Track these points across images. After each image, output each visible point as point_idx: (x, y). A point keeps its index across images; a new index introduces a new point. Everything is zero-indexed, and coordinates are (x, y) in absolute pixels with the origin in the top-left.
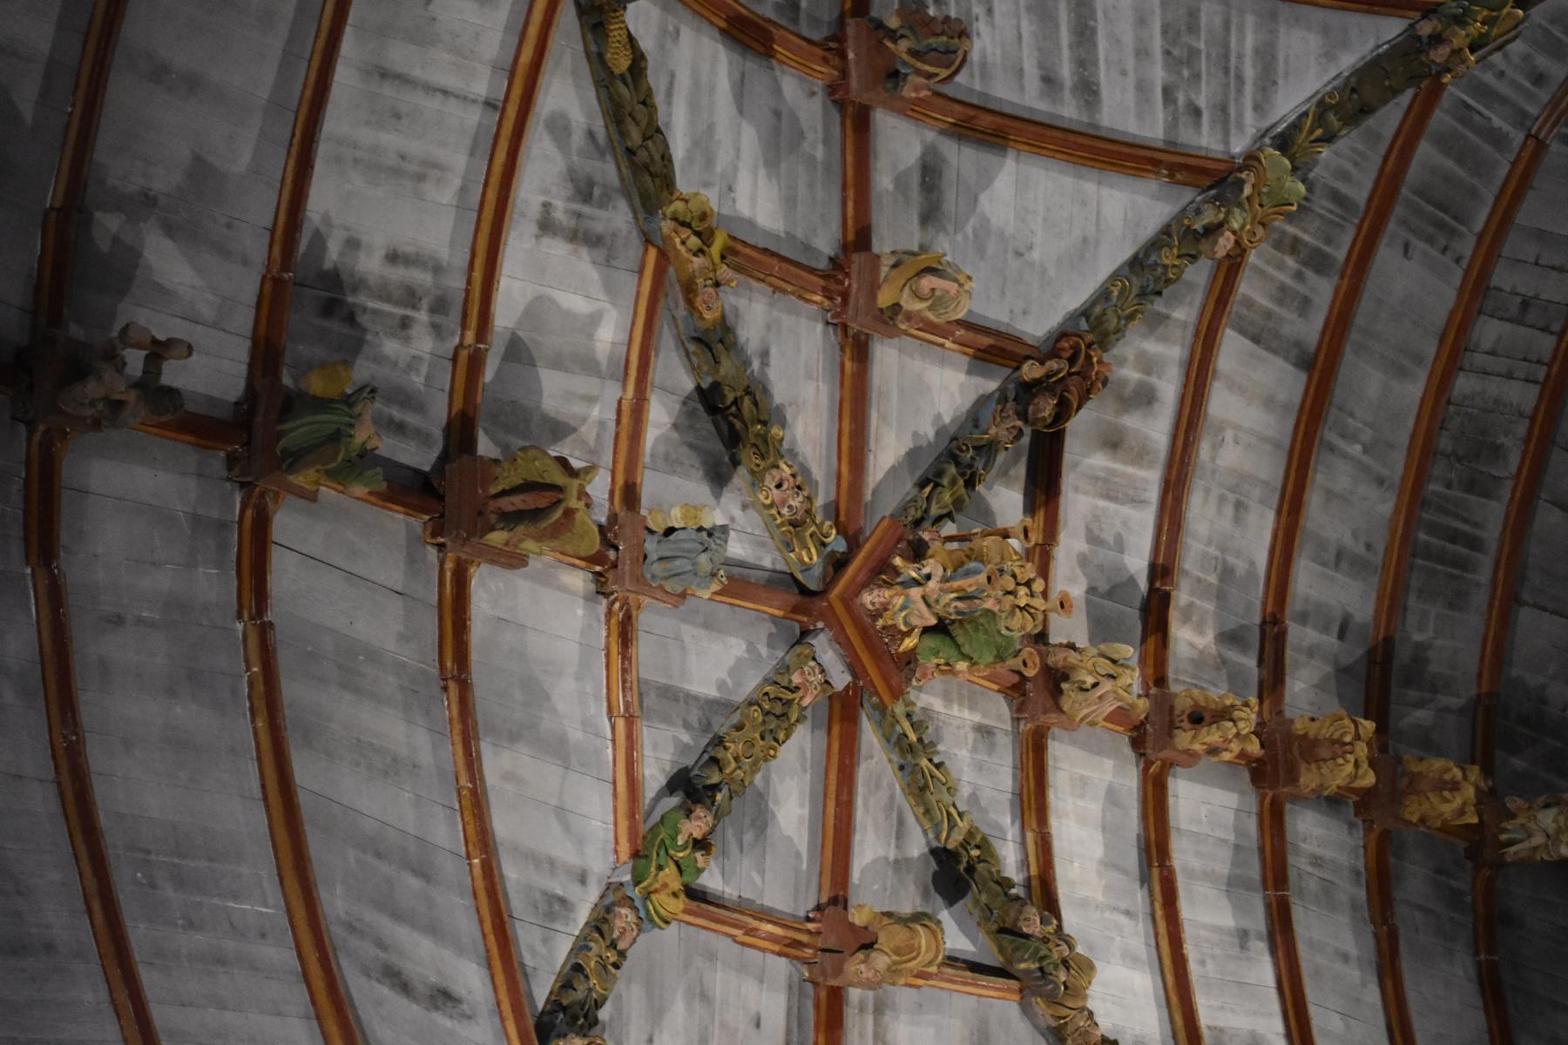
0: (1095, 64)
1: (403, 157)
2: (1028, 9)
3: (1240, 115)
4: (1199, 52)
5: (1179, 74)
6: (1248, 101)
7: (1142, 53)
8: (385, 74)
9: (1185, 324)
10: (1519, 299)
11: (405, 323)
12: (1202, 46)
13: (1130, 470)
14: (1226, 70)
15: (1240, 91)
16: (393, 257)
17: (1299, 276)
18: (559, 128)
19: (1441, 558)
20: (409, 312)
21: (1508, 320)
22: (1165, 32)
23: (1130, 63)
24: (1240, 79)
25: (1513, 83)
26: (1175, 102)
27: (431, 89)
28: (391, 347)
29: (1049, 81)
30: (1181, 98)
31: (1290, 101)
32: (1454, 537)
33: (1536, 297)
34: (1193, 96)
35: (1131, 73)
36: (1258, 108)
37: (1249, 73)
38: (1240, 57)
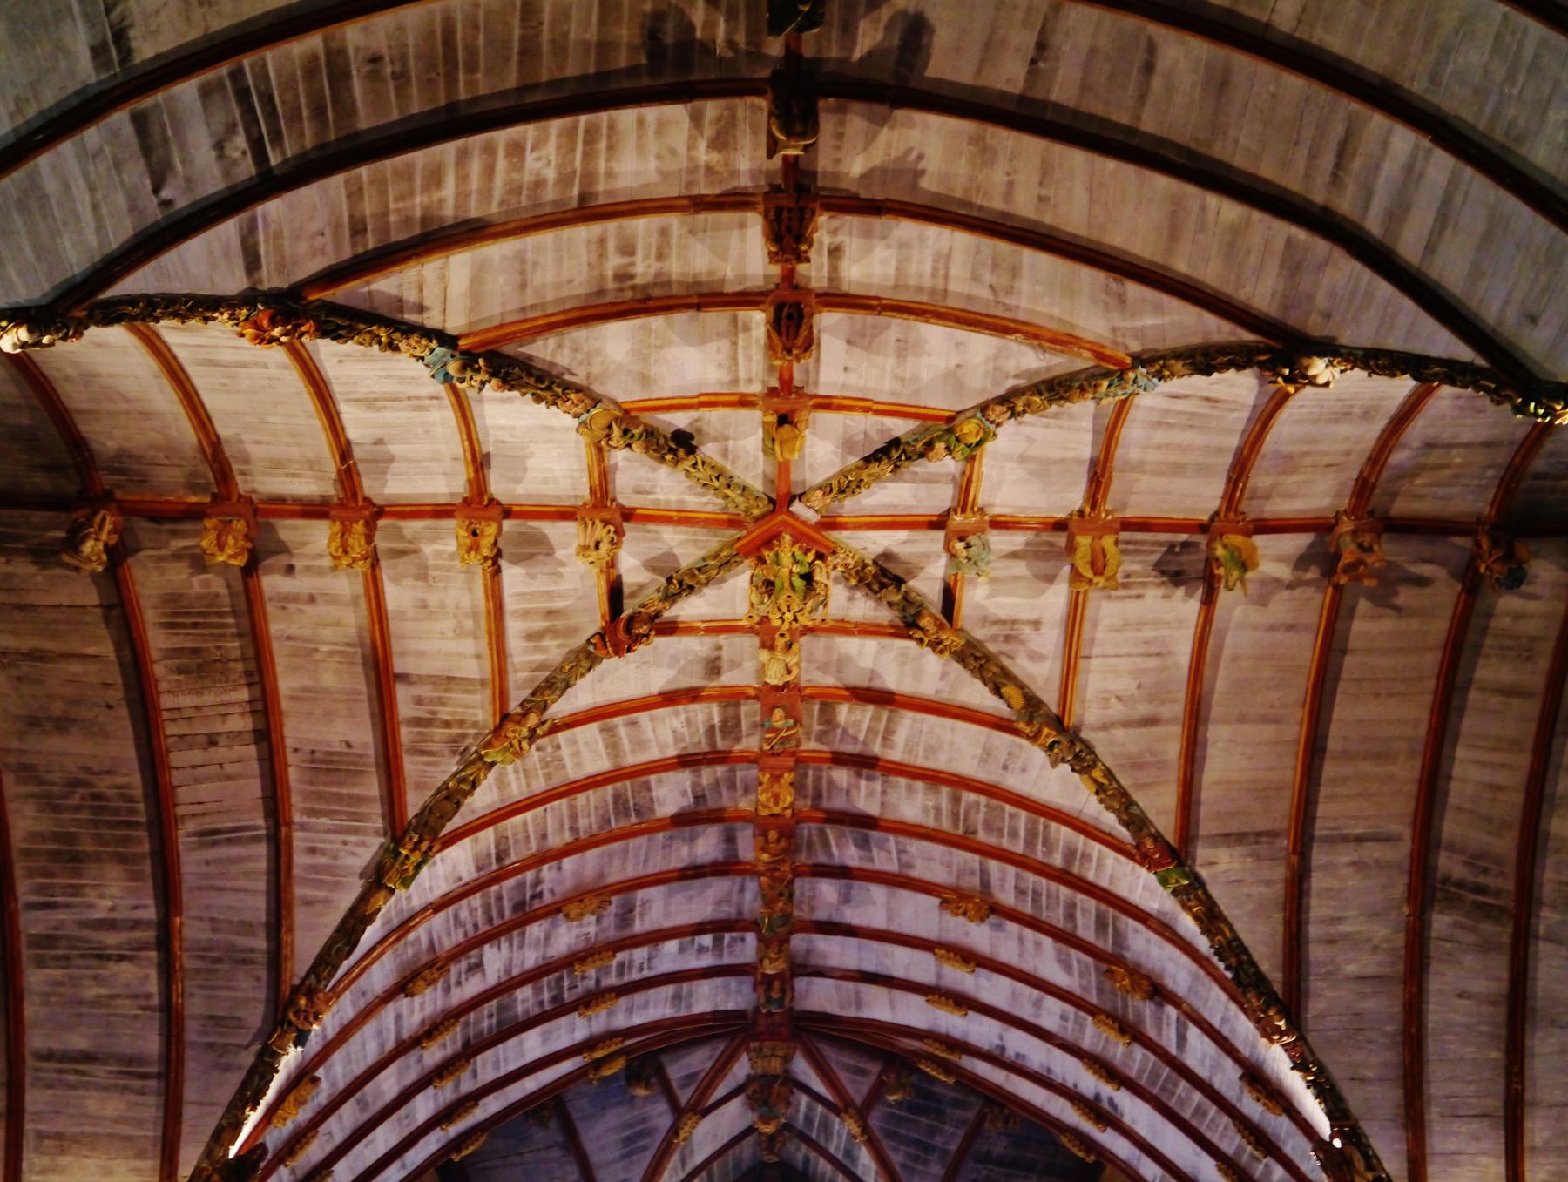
7: (577, 754)
8: (1158, 655)
9: (516, 671)
17: (433, 713)
18: (1035, 656)
19: (188, 614)
25: (331, 842)
27: (1130, 655)
28: (1136, 567)
32: (183, 626)
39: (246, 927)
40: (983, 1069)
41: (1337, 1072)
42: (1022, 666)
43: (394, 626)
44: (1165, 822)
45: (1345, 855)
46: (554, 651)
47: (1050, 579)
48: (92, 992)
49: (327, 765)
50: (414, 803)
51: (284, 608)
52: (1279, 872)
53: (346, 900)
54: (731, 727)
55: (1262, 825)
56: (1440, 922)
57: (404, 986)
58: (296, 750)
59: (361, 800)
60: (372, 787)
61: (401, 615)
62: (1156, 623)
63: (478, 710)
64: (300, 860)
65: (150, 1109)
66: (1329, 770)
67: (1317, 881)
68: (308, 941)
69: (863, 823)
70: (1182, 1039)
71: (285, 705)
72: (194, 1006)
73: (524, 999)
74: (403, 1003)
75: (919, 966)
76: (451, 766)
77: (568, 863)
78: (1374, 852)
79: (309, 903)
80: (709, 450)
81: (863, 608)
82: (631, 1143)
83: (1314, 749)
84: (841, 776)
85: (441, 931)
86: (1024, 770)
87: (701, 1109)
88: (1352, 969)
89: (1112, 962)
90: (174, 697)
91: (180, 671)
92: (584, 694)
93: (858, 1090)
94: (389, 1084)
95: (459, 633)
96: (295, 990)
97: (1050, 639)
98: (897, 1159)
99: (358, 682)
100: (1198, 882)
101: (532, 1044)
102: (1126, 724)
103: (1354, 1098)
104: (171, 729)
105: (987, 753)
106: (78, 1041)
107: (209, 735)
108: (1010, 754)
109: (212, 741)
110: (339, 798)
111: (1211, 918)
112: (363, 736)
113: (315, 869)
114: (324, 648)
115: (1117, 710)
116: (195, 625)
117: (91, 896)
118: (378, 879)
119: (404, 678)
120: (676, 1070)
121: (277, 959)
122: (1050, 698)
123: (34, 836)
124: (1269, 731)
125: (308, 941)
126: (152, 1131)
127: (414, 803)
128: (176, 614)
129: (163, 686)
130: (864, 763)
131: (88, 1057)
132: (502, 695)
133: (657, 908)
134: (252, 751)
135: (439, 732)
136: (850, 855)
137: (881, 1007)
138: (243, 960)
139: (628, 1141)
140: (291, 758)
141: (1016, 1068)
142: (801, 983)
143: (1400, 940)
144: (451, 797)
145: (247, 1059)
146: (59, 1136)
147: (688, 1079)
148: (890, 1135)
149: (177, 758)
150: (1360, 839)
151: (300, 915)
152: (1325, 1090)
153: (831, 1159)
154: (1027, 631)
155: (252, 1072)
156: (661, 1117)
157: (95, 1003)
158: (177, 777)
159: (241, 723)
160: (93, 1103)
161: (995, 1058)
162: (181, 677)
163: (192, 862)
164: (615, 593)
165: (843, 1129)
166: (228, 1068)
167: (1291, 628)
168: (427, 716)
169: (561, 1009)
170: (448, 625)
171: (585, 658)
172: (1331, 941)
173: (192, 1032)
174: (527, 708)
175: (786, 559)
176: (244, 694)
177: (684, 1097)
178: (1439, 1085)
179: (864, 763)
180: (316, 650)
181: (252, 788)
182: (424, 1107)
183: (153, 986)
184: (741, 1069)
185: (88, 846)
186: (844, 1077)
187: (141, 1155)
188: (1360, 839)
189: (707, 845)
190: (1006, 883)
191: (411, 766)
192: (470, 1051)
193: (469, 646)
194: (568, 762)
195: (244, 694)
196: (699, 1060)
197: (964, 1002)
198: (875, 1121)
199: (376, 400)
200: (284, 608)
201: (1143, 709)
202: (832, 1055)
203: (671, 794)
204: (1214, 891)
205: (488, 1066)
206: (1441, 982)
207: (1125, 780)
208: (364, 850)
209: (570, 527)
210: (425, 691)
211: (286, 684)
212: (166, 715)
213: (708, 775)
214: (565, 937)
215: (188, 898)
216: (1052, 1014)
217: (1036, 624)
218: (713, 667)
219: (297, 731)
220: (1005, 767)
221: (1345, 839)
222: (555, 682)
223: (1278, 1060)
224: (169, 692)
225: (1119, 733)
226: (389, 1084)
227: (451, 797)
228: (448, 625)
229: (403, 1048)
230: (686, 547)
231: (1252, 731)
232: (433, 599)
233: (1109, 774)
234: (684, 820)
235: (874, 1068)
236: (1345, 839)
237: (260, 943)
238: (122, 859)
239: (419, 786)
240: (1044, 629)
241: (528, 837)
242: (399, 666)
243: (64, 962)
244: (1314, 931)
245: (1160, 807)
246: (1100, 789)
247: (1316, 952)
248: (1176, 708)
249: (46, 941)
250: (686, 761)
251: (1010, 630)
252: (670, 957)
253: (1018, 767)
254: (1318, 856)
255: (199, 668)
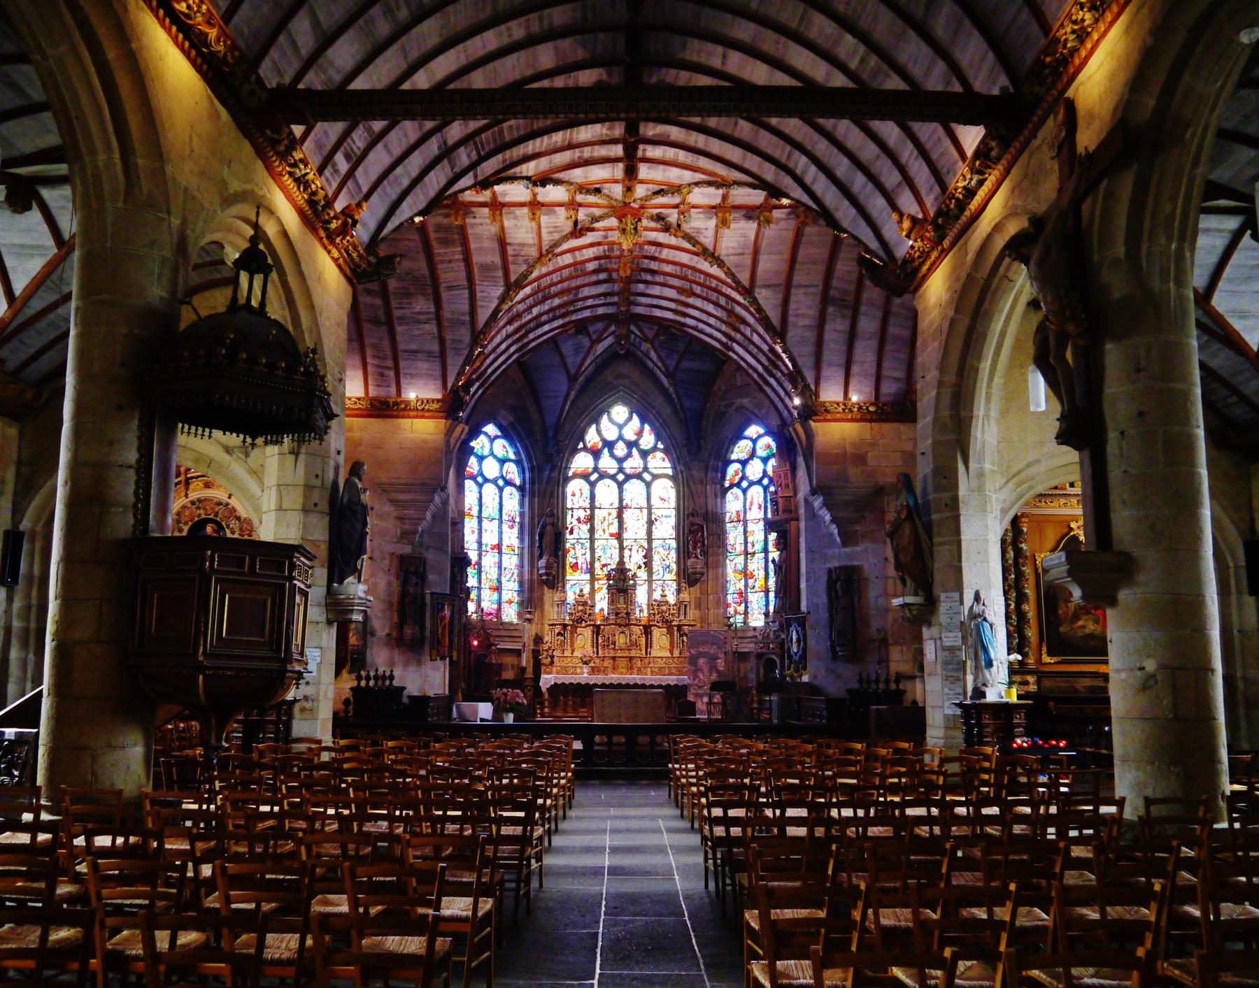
18: (705, 237)
39: (463, 314)
40: (690, 331)
41: (795, 354)
42: (702, 239)
43: (507, 231)
44: (746, 283)
45: (801, 291)
46: (556, 236)
47: (711, 218)
48: (416, 332)
49: (486, 268)
50: (513, 278)
52: (780, 296)
53: (494, 305)
54: (611, 250)
55: (776, 282)
56: (830, 310)
57: (510, 322)
59: (497, 277)
60: (500, 273)
61: (509, 228)
62: (744, 229)
63: (534, 252)
64: (479, 295)
65: (438, 366)
66: (797, 266)
67: (793, 298)
68: (483, 316)
69: (653, 272)
70: (752, 335)
71: (473, 251)
72: (449, 337)
73: (544, 318)
74: (508, 327)
75: (672, 305)
76: (524, 267)
77: (559, 286)
78: (810, 290)
79: (482, 307)
80: (605, 191)
81: (652, 224)
82: (578, 349)
83: (793, 261)
84: (646, 261)
85: (521, 307)
87: (599, 340)
88: (803, 323)
89: (731, 312)
90: (438, 250)
92: (565, 246)
93: (650, 334)
94: (503, 347)
95: (527, 232)
96: (480, 332)
97: (711, 233)
98: (663, 354)
99: (496, 245)
100: (755, 299)
101: (546, 328)
102: (734, 255)
103: (800, 361)
104: (437, 259)
105: (691, 259)
106: (414, 347)
109: (450, 262)
110: (489, 276)
111: (759, 309)
112: (497, 259)
113: (484, 297)
115: (731, 251)
117: (414, 305)
118: (503, 299)
119: (509, 244)
120: (591, 329)
121: (473, 322)
122: (711, 248)
123: (395, 288)
124: (779, 257)
125: (483, 316)
126: (438, 373)
127: (513, 278)
130: (654, 258)
131: (417, 352)
132: (540, 248)
133: (586, 292)
134: (462, 264)
135: (521, 258)
136: (649, 278)
137: (658, 313)
138: (462, 323)
139: (576, 349)
140: (475, 266)
141: (702, 332)
142: (632, 307)
143: (817, 314)
144: (525, 276)
145: (466, 352)
146: (411, 374)
147: (595, 332)
148: (661, 347)
149: (439, 266)
150: (807, 286)
151: (480, 311)
152: (791, 359)
153: (642, 352)
154: (703, 231)
155: (467, 356)
156: (586, 343)
157: (419, 335)
158: (439, 272)
159: (459, 257)
160: (420, 364)
161: (695, 328)
163: (445, 296)
164: (576, 223)
165: (645, 346)
166: (461, 355)
167: (786, 230)
169: (555, 318)
170: (524, 230)
171: (566, 238)
172: (797, 315)
173: (448, 344)
174: (548, 252)
175: (629, 221)
176: (460, 249)
177: (594, 337)
178: (827, 356)
179: (654, 258)
181: (463, 274)
182: (512, 349)
183: (435, 330)
184: (613, 328)
185: (412, 291)
186: (646, 331)
187: (436, 380)
188: (807, 286)
189: (602, 276)
190: (698, 289)
191: (512, 268)
192: (526, 335)
193: (530, 236)
195: (460, 249)
196: (600, 326)
197: (685, 315)
198: (656, 343)
201: (740, 251)
202: (641, 323)
203: (591, 266)
204: (761, 302)
205: (531, 336)
206: (829, 327)
207: (733, 270)
208: (498, 291)
209: (563, 209)
210: (517, 247)
211: (473, 246)
213: (603, 261)
214: (557, 301)
215: (445, 306)
216: (712, 321)
217: (707, 229)
218: (606, 237)
219: (476, 259)
221: (801, 286)
222: (556, 244)
223: (778, 348)
225: (732, 257)
226: (503, 347)
227: (525, 276)
228: (524, 230)
229: (508, 337)
230: (597, 212)
231: (773, 257)
232: (518, 224)
233: (729, 269)
234: (595, 272)
235: (656, 327)
236: (801, 286)
237: (467, 318)
238: (423, 295)
239: (515, 273)
242: (508, 241)
243: (408, 324)
244: (791, 312)
245: (744, 278)
246: (725, 273)
247: (791, 319)
248: (750, 250)
249: (401, 318)
250: (596, 258)
251: (698, 230)
252: (590, 302)
254: (793, 291)
255: (446, 242)
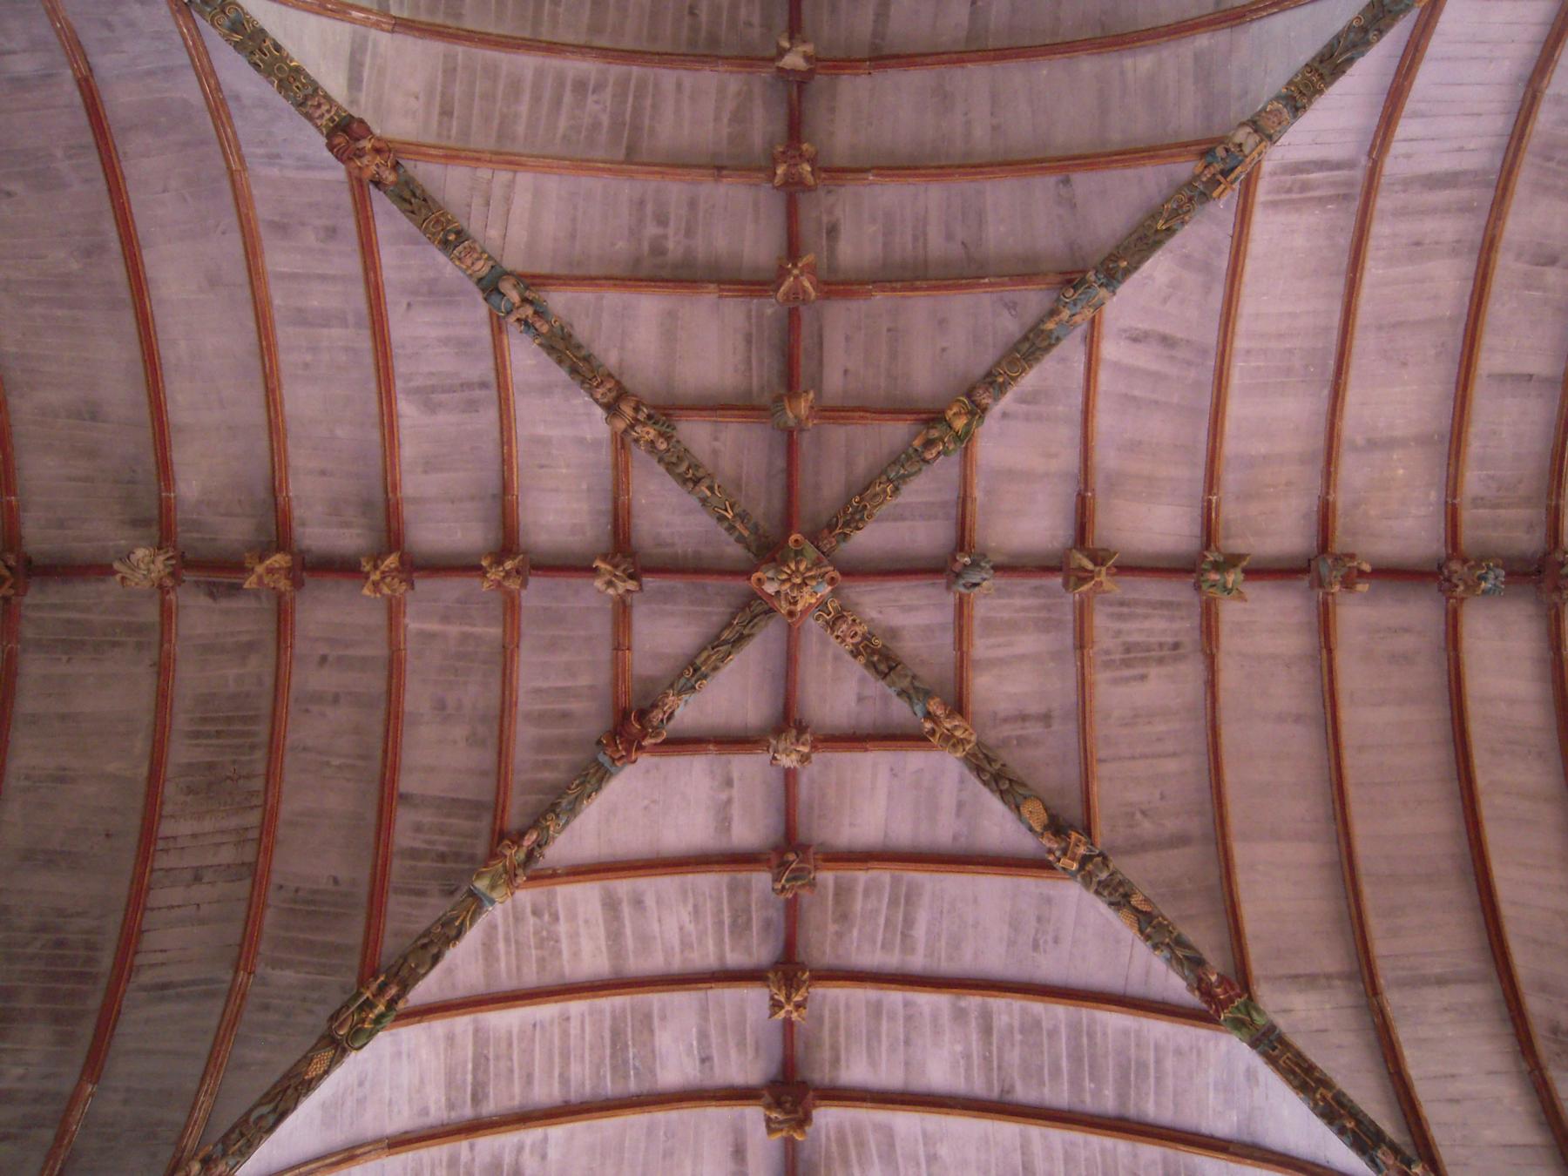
0: (605, 921)
1: (1149, 723)
2: (655, 938)
3: (506, 918)
4: (536, 948)
5: (549, 932)
6: (501, 930)
7: (574, 936)
10: (206, 879)
11: (1128, 650)
12: (534, 952)
13: (551, 707)
14: (517, 942)
15: (507, 934)
16: (1143, 677)
19: (213, 720)
20: (1127, 656)
21: (211, 866)
22: (560, 952)
23: (582, 930)
24: (507, 940)
26: (550, 915)
29: (638, 903)
30: (546, 917)
31: (473, 936)
32: (208, 735)
33: (188, 886)
34: (538, 921)
35: (581, 923)
36: (494, 927)
37: (501, 946)
38: (508, 953)
51: (307, 711)
58: (281, 887)
86: (1056, 941)
91: (190, 790)
107: (197, 869)
108: (1039, 919)
114: (336, 762)
116: (218, 734)
128: (204, 720)
129: (168, 809)
162: (189, 798)
168: (424, 846)
180: (328, 764)
191: (395, 904)
194: (566, 955)
199: (433, 389)
200: (307, 711)
212: (161, 844)
220: (1036, 947)
224: (172, 816)
240: (1056, 727)
241: (511, 1071)
253: (1049, 938)
